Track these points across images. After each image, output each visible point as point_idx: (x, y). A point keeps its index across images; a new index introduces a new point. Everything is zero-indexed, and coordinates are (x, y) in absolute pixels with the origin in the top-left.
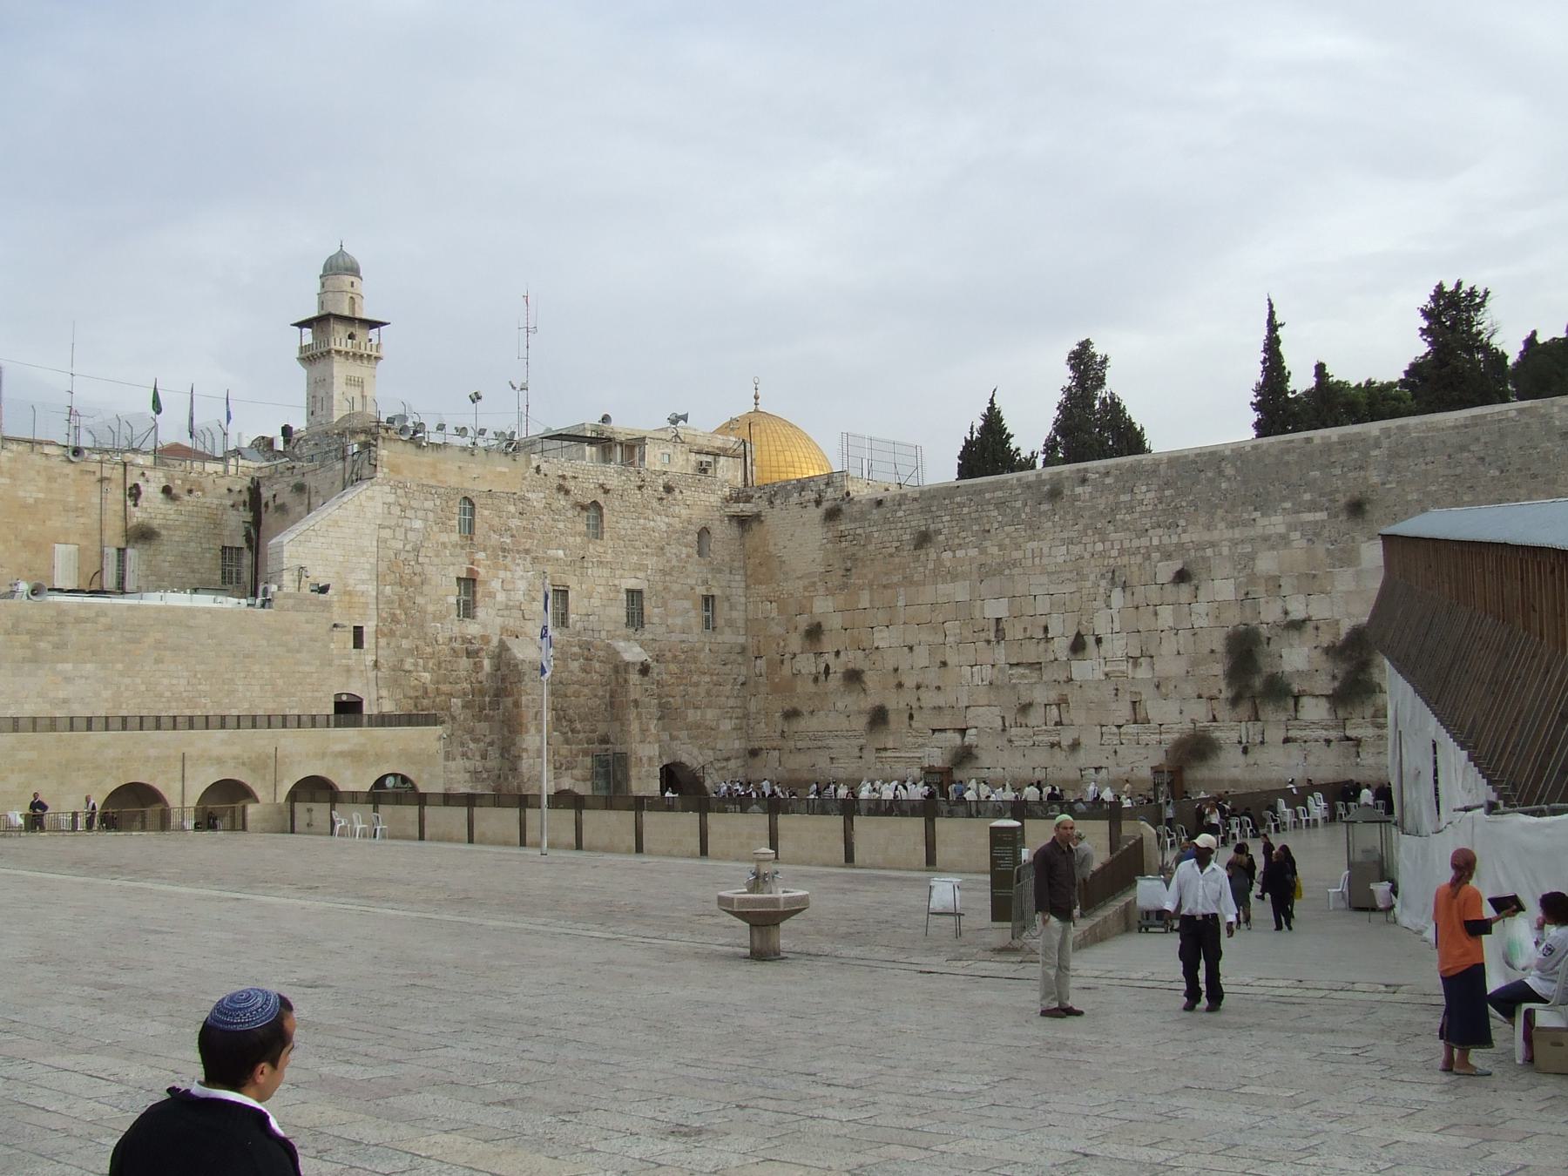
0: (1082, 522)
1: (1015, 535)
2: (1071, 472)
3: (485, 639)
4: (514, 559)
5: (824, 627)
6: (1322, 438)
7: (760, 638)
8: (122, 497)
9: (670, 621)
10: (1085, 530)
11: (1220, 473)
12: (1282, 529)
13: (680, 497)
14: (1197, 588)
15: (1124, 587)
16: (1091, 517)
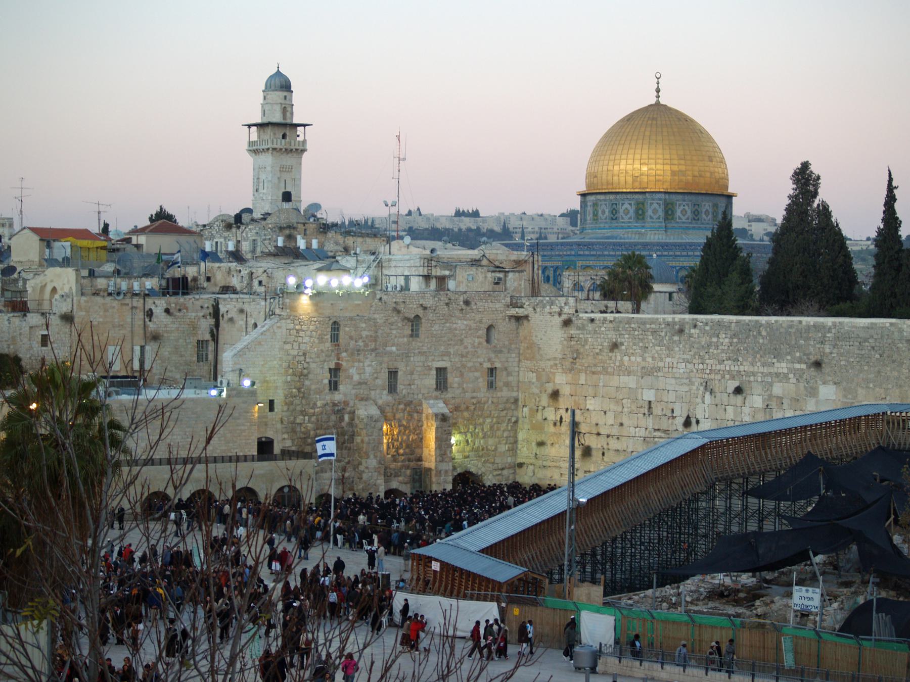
0: (694, 350)
1: (660, 352)
2: (690, 319)
3: (346, 403)
4: (365, 355)
5: (560, 393)
6: (807, 322)
7: (527, 394)
8: (142, 317)
9: (465, 386)
10: (694, 355)
11: (759, 333)
12: (785, 371)
13: (475, 307)
14: (745, 398)
15: (711, 393)
16: (697, 348)
